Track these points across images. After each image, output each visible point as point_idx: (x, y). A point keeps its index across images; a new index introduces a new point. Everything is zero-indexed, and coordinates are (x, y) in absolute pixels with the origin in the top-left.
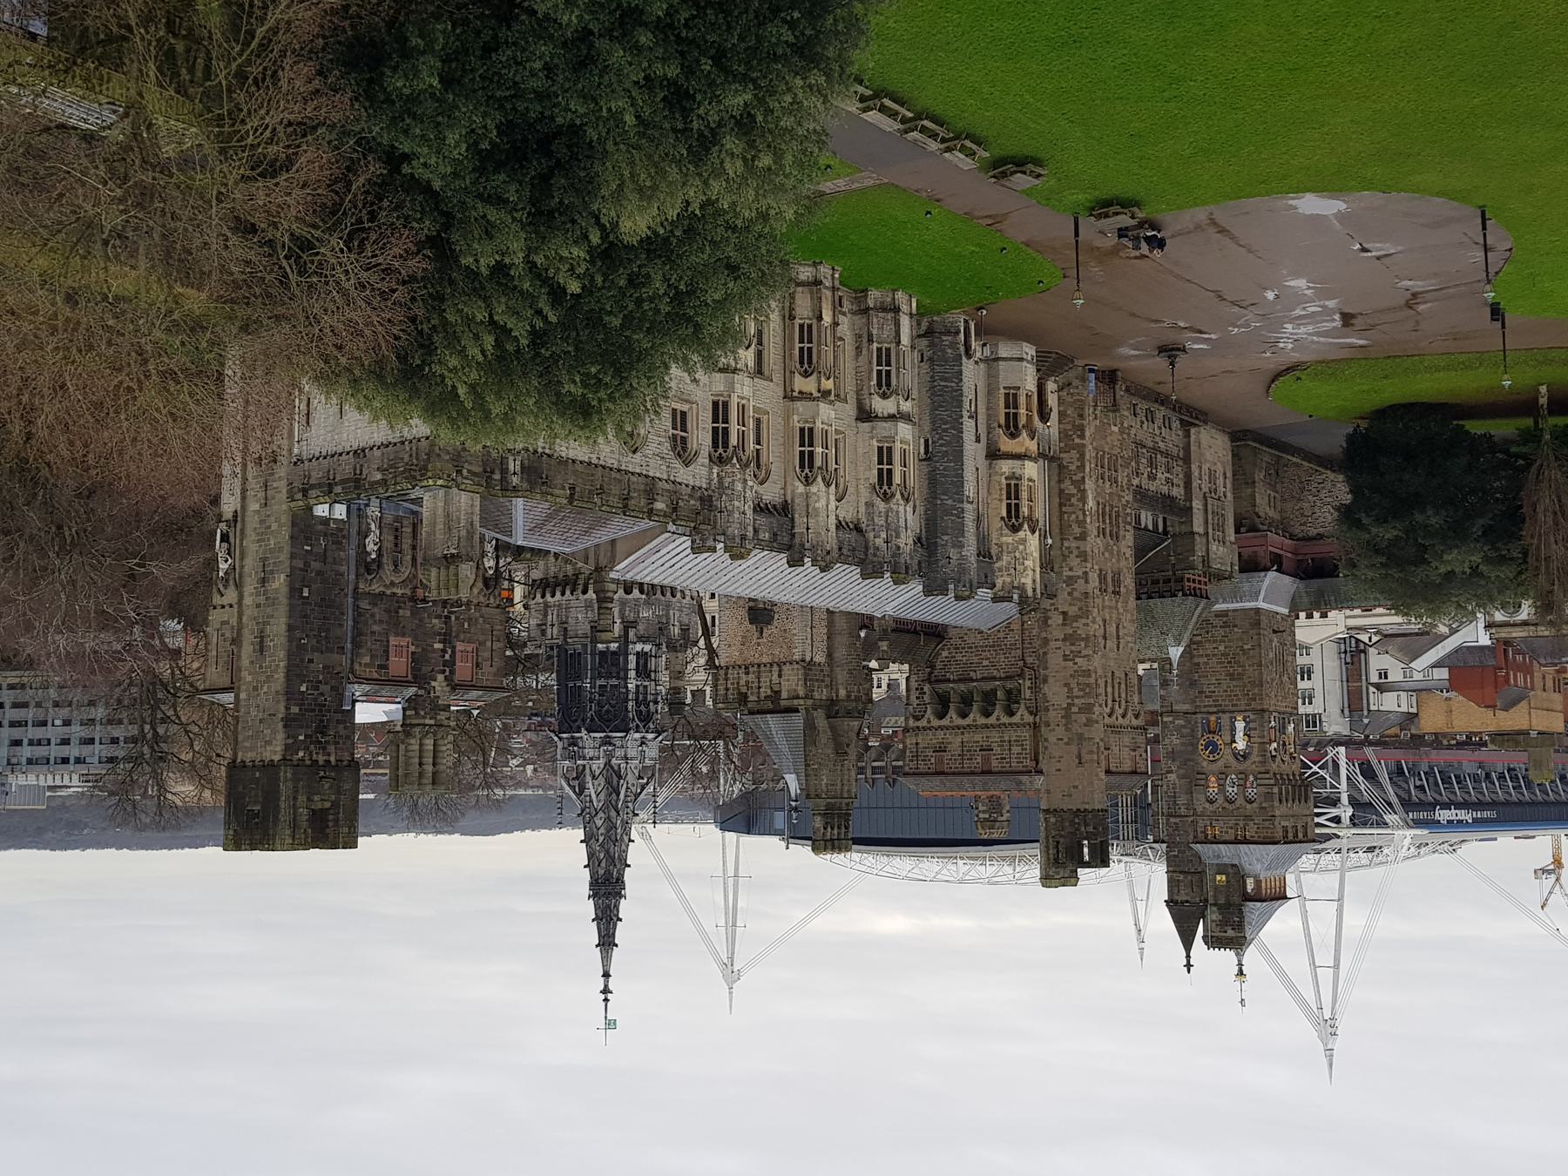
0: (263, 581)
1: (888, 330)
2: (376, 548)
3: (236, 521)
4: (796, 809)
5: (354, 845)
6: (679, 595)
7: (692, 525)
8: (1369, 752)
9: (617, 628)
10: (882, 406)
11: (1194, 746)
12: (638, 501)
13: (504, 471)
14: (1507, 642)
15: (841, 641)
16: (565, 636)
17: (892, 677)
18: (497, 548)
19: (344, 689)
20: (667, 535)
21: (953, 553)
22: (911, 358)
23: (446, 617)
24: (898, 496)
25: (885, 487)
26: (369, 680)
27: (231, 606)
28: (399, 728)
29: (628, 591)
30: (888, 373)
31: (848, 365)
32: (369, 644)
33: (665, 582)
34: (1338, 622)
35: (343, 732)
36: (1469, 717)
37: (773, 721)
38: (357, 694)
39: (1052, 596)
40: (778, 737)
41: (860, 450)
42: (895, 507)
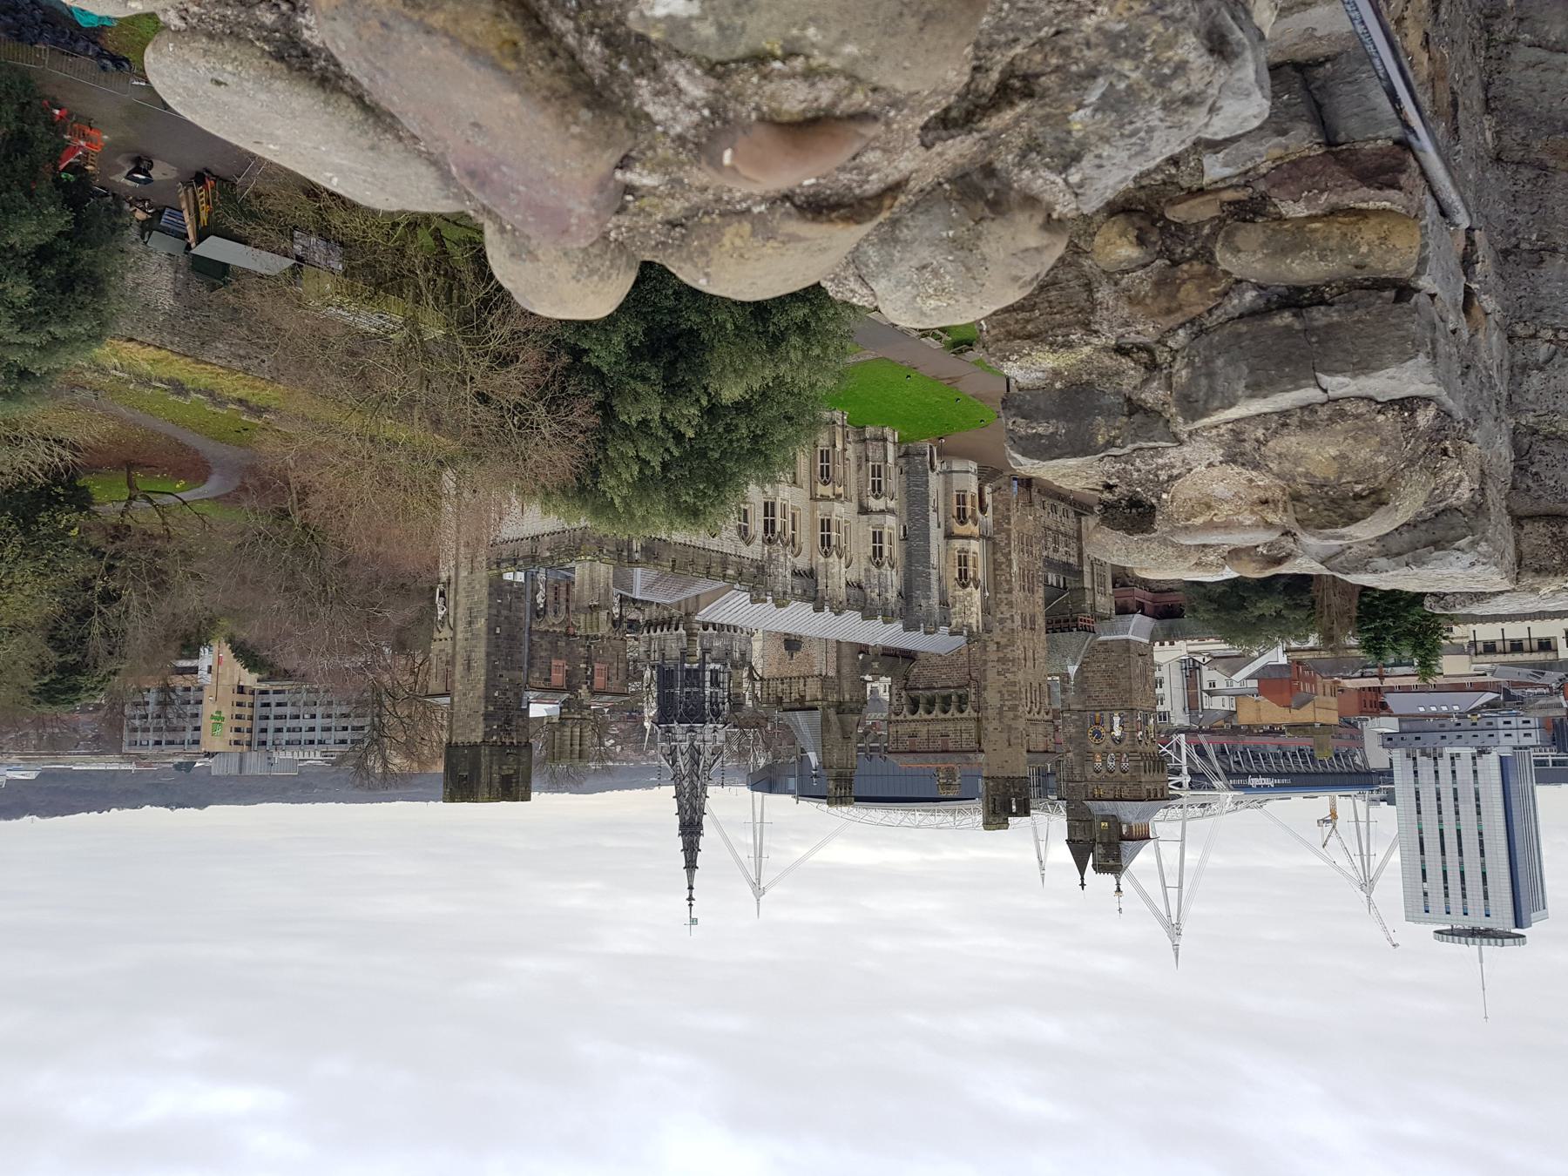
1: (879, 454)
4: (815, 776)
5: (528, 799)
8: (1202, 738)
9: (698, 653)
10: (874, 504)
12: (716, 569)
13: (630, 550)
14: (1299, 663)
15: (846, 661)
17: (882, 687)
21: (923, 602)
22: (894, 472)
29: (705, 628)
30: (879, 482)
31: (852, 477)
34: (1182, 648)
36: (1273, 713)
37: (800, 717)
39: (989, 631)
40: (804, 728)
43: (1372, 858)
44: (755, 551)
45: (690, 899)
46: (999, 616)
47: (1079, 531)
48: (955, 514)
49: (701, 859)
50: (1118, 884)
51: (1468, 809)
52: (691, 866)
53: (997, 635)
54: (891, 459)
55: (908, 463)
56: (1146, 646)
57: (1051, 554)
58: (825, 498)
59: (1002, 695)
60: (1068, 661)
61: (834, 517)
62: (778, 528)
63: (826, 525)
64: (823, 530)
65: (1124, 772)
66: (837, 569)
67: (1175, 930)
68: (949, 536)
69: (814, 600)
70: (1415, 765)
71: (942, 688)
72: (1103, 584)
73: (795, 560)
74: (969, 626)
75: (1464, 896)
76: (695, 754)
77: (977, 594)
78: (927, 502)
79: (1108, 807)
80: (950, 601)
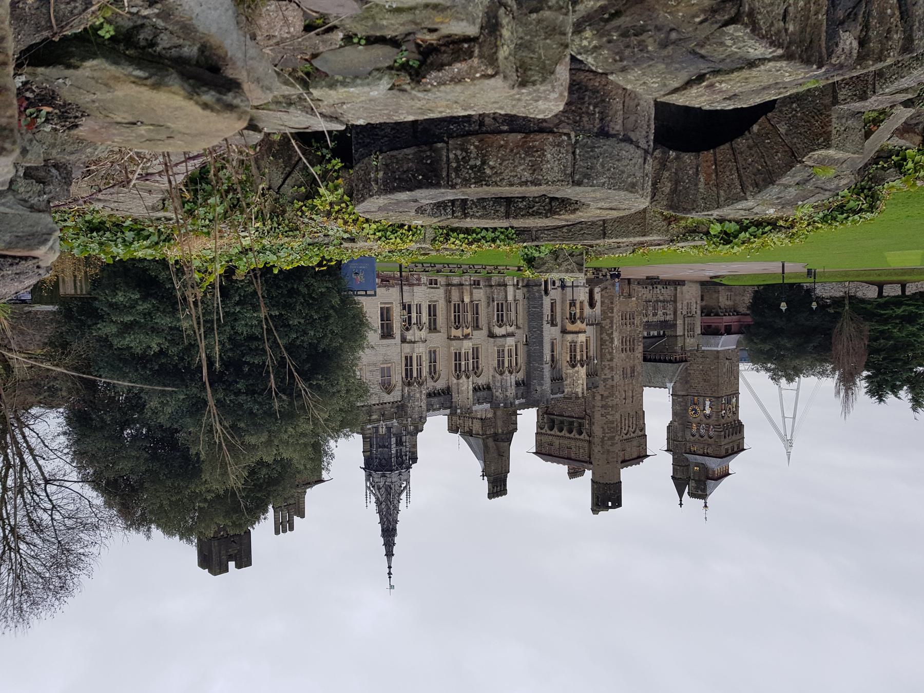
1: (502, 294)
10: (498, 331)
11: (687, 410)
21: (538, 388)
24: (507, 372)
44: (396, 396)
45: (390, 573)
46: (603, 377)
47: (676, 295)
48: (568, 316)
49: (395, 550)
50: (706, 503)
52: (389, 554)
53: (601, 389)
55: (528, 291)
57: (651, 319)
58: (457, 338)
59: (604, 430)
60: (667, 380)
61: (463, 351)
62: (415, 375)
63: (458, 356)
65: (711, 438)
66: (466, 387)
68: (564, 331)
69: (450, 408)
71: (568, 417)
72: (692, 329)
73: (435, 384)
74: (577, 393)
76: (388, 489)
77: (582, 371)
78: (542, 319)
79: (700, 459)
80: (564, 376)
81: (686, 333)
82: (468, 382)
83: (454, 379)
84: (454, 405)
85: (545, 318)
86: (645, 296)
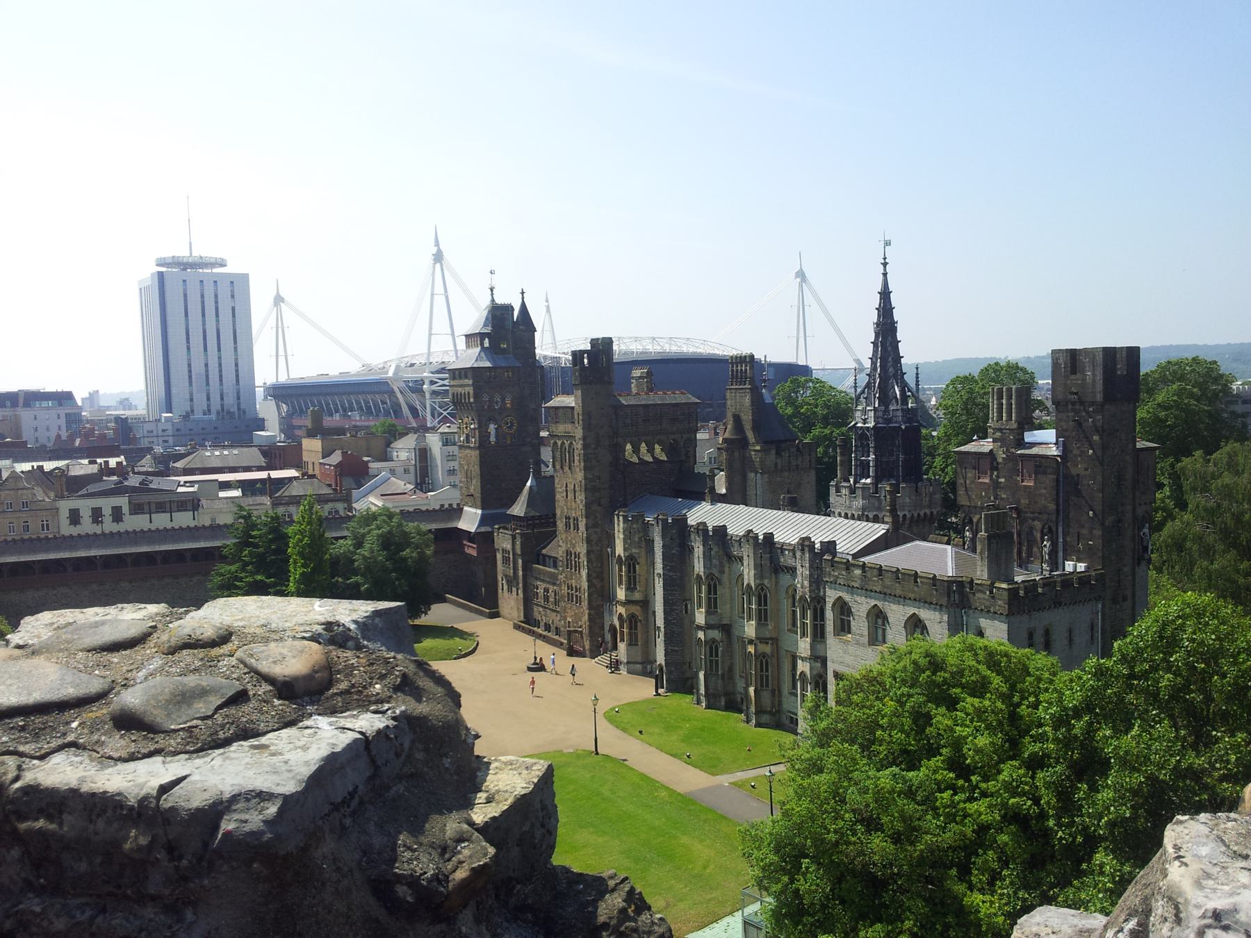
0: (1119, 521)
2: (1045, 543)
3: (1138, 559)
6: (843, 515)
7: (836, 559)
16: (917, 487)
18: (964, 543)
19: (1064, 451)
20: (851, 553)
23: (997, 499)
25: (712, 583)
26: (1046, 457)
27: (1140, 505)
28: (1026, 426)
30: (711, 656)
32: (1048, 481)
33: (853, 522)
35: (1063, 424)
38: (1055, 449)
41: (728, 606)
42: (706, 571)
43: (274, 326)
45: (885, 264)
48: (639, 624)
50: (492, 295)
51: (198, 368)
52: (885, 294)
54: (701, 675)
56: (466, 504)
57: (551, 588)
63: (762, 618)
64: (766, 610)
67: (438, 257)
68: (646, 604)
70: (239, 404)
75: (202, 296)
76: (885, 398)
77: (619, 550)
78: (665, 634)
81: (511, 556)
82: (749, 579)
83: (768, 585)
84: (768, 550)
85: (662, 635)
86: (558, 618)
